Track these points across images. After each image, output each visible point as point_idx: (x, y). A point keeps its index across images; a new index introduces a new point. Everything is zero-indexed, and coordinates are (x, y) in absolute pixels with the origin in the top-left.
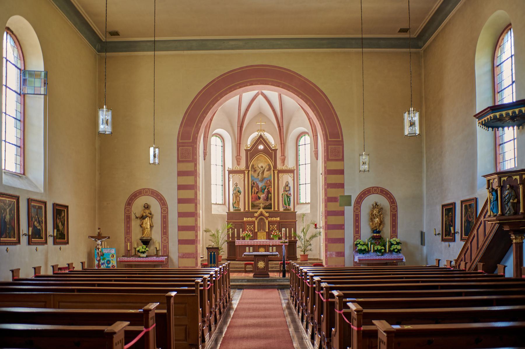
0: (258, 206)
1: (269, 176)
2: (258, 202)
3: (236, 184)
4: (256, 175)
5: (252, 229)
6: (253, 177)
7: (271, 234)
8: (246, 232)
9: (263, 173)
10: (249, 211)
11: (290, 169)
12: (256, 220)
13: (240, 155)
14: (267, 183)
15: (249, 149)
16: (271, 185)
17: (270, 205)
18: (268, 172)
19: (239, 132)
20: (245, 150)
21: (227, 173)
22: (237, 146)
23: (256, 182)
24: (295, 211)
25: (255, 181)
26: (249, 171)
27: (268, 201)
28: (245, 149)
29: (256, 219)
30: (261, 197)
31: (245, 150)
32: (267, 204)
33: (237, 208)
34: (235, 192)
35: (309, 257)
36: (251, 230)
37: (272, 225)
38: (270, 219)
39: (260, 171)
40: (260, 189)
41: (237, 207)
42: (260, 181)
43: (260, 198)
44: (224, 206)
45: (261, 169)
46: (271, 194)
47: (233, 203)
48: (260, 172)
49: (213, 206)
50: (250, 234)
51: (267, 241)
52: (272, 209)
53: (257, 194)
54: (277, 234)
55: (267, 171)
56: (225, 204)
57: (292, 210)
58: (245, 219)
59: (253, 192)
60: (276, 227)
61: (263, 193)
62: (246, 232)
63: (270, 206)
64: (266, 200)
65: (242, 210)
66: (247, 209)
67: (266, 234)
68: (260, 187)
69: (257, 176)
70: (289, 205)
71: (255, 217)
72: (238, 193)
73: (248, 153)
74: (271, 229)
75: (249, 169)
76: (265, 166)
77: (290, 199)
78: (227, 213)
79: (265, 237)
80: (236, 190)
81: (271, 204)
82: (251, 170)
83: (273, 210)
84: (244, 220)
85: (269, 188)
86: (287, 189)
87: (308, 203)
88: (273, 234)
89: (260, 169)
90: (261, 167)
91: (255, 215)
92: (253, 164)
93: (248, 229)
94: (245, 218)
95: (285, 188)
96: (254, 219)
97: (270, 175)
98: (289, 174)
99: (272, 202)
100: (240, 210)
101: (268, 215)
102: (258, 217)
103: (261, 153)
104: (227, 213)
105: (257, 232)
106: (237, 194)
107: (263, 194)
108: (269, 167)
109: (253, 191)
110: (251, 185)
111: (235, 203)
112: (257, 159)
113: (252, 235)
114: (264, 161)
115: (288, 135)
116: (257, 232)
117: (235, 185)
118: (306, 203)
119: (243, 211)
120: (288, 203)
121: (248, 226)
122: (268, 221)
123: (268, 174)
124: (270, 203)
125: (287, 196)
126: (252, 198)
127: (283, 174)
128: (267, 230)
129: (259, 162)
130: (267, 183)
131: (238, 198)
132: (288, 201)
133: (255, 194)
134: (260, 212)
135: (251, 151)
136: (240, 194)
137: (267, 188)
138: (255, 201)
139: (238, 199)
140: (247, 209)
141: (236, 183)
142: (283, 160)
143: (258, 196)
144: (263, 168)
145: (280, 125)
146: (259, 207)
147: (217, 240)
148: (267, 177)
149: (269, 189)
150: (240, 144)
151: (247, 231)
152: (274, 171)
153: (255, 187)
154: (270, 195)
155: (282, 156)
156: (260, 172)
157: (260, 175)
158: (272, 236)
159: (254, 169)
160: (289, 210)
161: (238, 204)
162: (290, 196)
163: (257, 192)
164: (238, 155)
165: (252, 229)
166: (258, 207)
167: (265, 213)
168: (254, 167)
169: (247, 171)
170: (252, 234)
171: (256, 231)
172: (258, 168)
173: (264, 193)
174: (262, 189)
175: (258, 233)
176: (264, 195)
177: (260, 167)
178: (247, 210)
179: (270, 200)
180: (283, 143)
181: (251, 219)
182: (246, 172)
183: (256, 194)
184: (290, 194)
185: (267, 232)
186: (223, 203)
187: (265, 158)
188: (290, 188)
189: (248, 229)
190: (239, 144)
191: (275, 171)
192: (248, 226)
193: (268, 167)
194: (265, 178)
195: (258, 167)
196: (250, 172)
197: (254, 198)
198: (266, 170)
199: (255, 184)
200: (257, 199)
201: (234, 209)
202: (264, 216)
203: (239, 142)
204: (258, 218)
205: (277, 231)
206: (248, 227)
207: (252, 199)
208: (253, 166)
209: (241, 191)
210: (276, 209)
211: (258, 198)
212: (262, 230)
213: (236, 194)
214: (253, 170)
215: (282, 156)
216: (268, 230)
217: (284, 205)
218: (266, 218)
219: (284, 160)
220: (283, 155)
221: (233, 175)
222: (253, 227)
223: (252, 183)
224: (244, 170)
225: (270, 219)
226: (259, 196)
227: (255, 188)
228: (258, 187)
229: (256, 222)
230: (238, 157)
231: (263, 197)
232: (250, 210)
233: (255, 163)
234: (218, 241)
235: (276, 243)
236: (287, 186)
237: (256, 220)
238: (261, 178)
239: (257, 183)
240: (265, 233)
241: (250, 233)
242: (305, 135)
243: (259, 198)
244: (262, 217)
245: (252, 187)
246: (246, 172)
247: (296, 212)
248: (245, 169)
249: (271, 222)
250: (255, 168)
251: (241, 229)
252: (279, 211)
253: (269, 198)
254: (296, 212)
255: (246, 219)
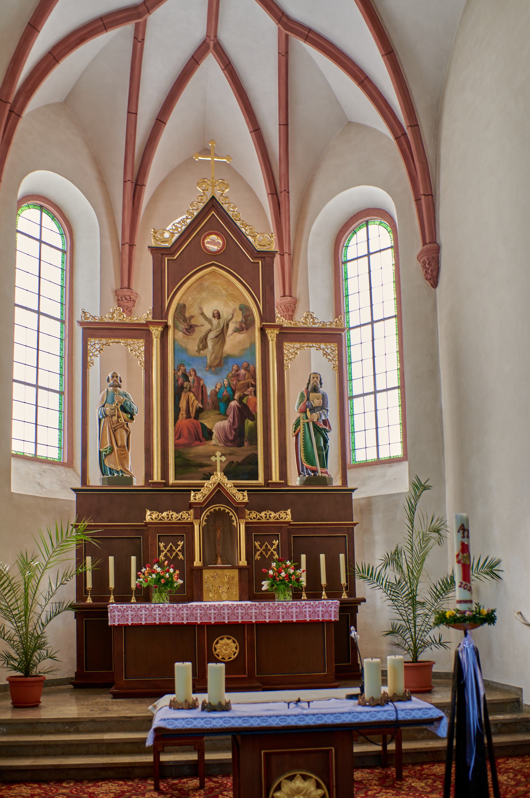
0: (202, 465)
1: (244, 350)
2: (201, 449)
3: (113, 377)
4: (192, 345)
5: (181, 557)
6: (185, 350)
7: (266, 577)
8: (155, 567)
9: (221, 336)
10: (166, 484)
11: (323, 325)
12: (195, 518)
13: (133, 286)
14: (237, 376)
15: (167, 245)
16: (254, 386)
17: (250, 464)
18: (240, 337)
19: (131, 204)
20: (153, 249)
21: (79, 331)
22: (121, 254)
23: (195, 371)
24: (350, 486)
25: (188, 369)
26: (166, 327)
27: (241, 445)
28: (153, 245)
29: (197, 516)
30: (213, 431)
31: (153, 249)
32: (240, 459)
33: (118, 472)
34: (108, 409)
35: (435, 669)
36: (175, 563)
37: (262, 538)
38: (253, 516)
39: (210, 331)
40: (209, 400)
41: (119, 468)
42: (210, 367)
43: (211, 433)
44: (67, 470)
45: (215, 321)
46: (253, 418)
47: (100, 452)
48: (211, 335)
49: (14, 463)
50: (171, 575)
51: (250, 607)
52: (256, 478)
53: (197, 417)
54: (288, 576)
55: (238, 330)
56: (69, 464)
57: (337, 483)
58: (150, 516)
59: (183, 414)
60: (277, 550)
61: (222, 417)
62: (155, 567)
63: (250, 467)
64: (232, 441)
65: (138, 481)
66: (157, 477)
67: (237, 579)
68: (209, 393)
69: (196, 349)
70: (324, 465)
71: (191, 506)
72: (121, 414)
73: (162, 261)
74: (257, 557)
75: (166, 317)
76: (230, 312)
77: (326, 441)
78: (75, 490)
79: (235, 591)
80: (113, 401)
81: (253, 460)
82: (175, 327)
83: (261, 480)
84: (148, 519)
85: (245, 395)
86: (317, 402)
87: (391, 461)
88: (274, 578)
89: (210, 322)
90: (214, 316)
91: (192, 500)
92: (181, 302)
93: (162, 557)
94: (148, 513)
95: (308, 399)
96: (187, 516)
97: (248, 345)
98: (323, 346)
99: (256, 449)
100: (129, 481)
101: (246, 500)
102: (207, 506)
103: (213, 264)
104: (75, 490)
105: (200, 570)
106: (119, 417)
107: (222, 420)
108: (245, 317)
109: (183, 404)
110: (176, 381)
111: (110, 453)
112: (200, 286)
113: (180, 582)
114: (224, 292)
115: (307, 222)
116: (200, 570)
117: (111, 382)
118: (379, 462)
119: (142, 484)
120: (319, 455)
121: (162, 545)
122: (247, 523)
123: (239, 342)
124: (249, 453)
125: (317, 430)
126: (178, 435)
127: (297, 345)
128: (243, 562)
129: (204, 295)
130: (237, 376)
131: (121, 434)
132: (319, 448)
133: (188, 416)
134: (212, 487)
135: (173, 254)
136: (132, 418)
137: (236, 396)
138: (189, 446)
139: (122, 439)
140: (157, 477)
141: (114, 376)
142: (288, 311)
143: (202, 425)
144: (222, 322)
145: (276, 190)
146: (206, 469)
147: (21, 602)
148: (236, 352)
149: (244, 401)
150: (132, 246)
151: (157, 562)
152: (262, 330)
153: (190, 390)
154: (249, 423)
155: (284, 295)
156: (211, 335)
157: (210, 344)
158: (266, 585)
159: (185, 320)
160: (326, 485)
161: (123, 458)
162: (327, 428)
163: (199, 411)
164: (126, 284)
165: (181, 557)
166: (201, 470)
167: (234, 491)
168: (187, 315)
169: (160, 329)
170: (181, 577)
171: (197, 563)
172: (201, 320)
173: (225, 416)
174: (219, 400)
175: (207, 574)
176: (225, 423)
177: (209, 314)
178: (159, 480)
179: (250, 444)
180: (286, 250)
181: (175, 515)
182: (156, 332)
183: (192, 420)
184: (325, 422)
185: (241, 569)
186: (66, 461)
187: (229, 281)
188: (324, 397)
189: (162, 557)
190: (127, 246)
191: (268, 331)
192: (162, 545)
193: (239, 317)
194: (228, 357)
195: (203, 314)
196: (171, 332)
197: (185, 432)
198: (232, 326)
199: (191, 379)
200: (198, 439)
201: (105, 477)
202: (228, 503)
203: (127, 240)
204: (202, 510)
205: (288, 563)
206: (162, 548)
207: (180, 437)
208: (182, 308)
209: (135, 407)
210: (275, 477)
211: (201, 435)
212: (219, 560)
213: (115, 418)
214: (183, 326)
215: (284, 295)
216: (247, 559)
217: (306, 465)
218: (236, 509)
219: (293, 311)
220: (287, 293)
221: (104, 341)
222: (181, 551)
223: (180, 373)
224: (148, 323)
225: (253, 514)
226: (208, 425)
227: (192, 394)
228: (203, 389)
229: (196, 527)
230: (126, 292)
231: (224, 428)
232: (172, 480)
233: (190, 299)
234: (26, 605)
235: (287, 613)
236: (315, 390)
237: (195, 518)
238: (216, 358)
239: (199, 374)
240: (236, 573)
241: (171, 570)
242: (367, 222)
243: (208, 434)
244: (222, 507)
245: (179, 391)
246: (156, 332)
247: (353, 490)
248: (150, 319)
249: (257, 529)
250: (192, 317)
251: (133, 559)
252: (286, 484)
253: (246, 434)
254: (353, 490)
255: (154, 516)
